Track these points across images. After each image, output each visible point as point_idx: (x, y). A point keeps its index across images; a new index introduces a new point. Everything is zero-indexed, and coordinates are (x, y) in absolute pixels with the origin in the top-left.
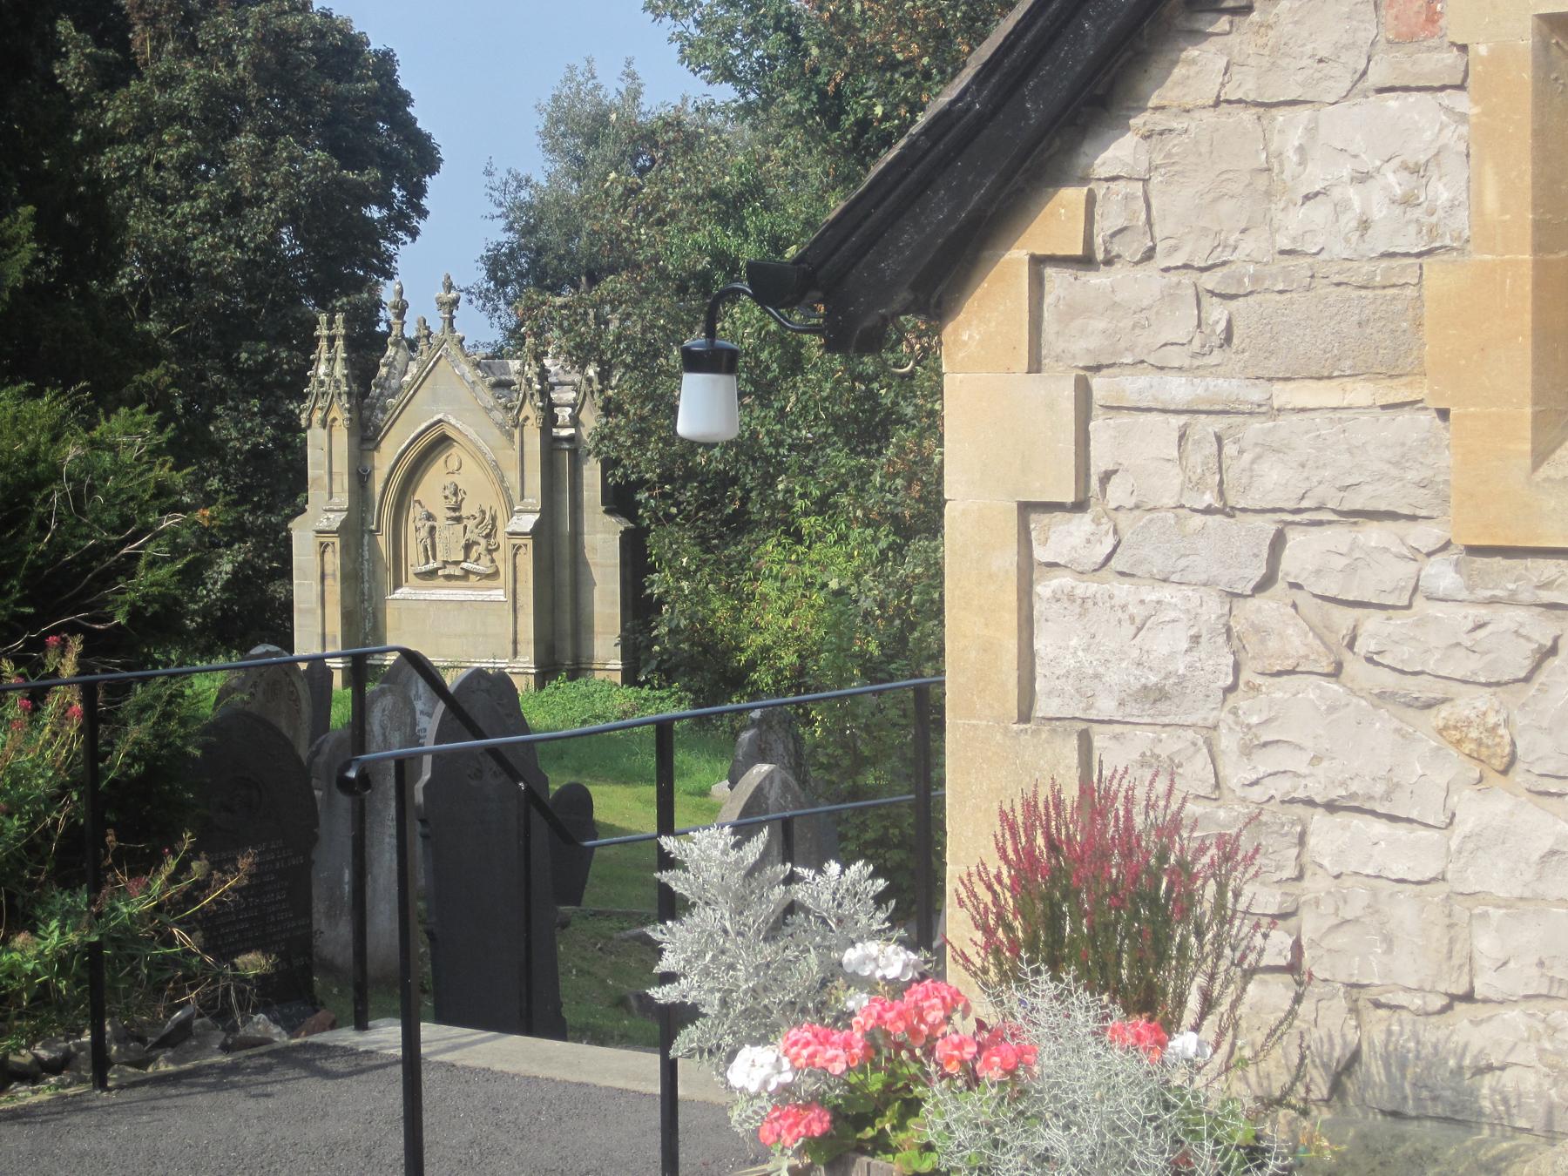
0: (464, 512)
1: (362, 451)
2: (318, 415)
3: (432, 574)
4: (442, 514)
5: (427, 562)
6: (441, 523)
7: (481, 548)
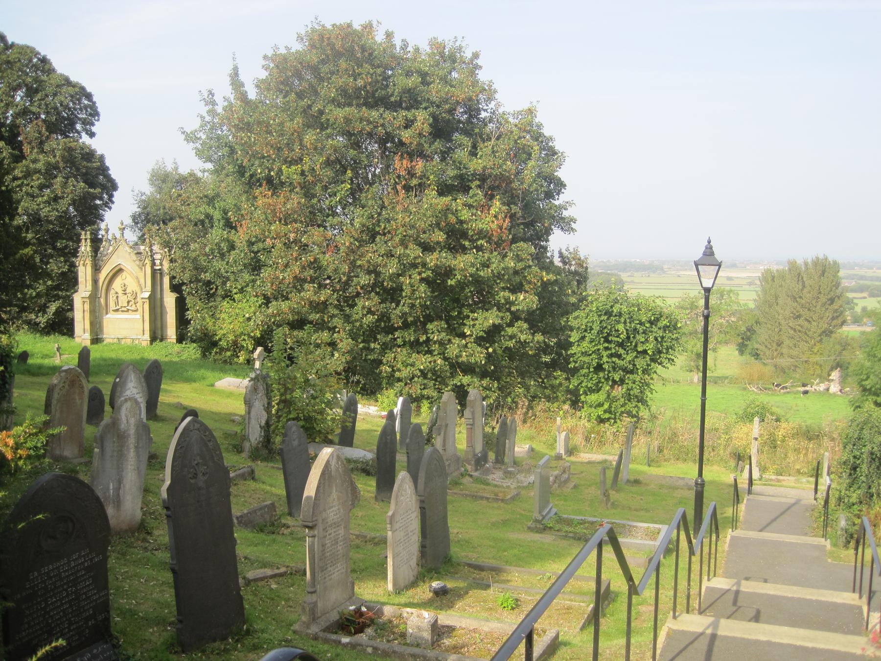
2: (82, 262)
3: (117, 310)
4: (120, 292)
6: (120, 295)
7: (132, 303)
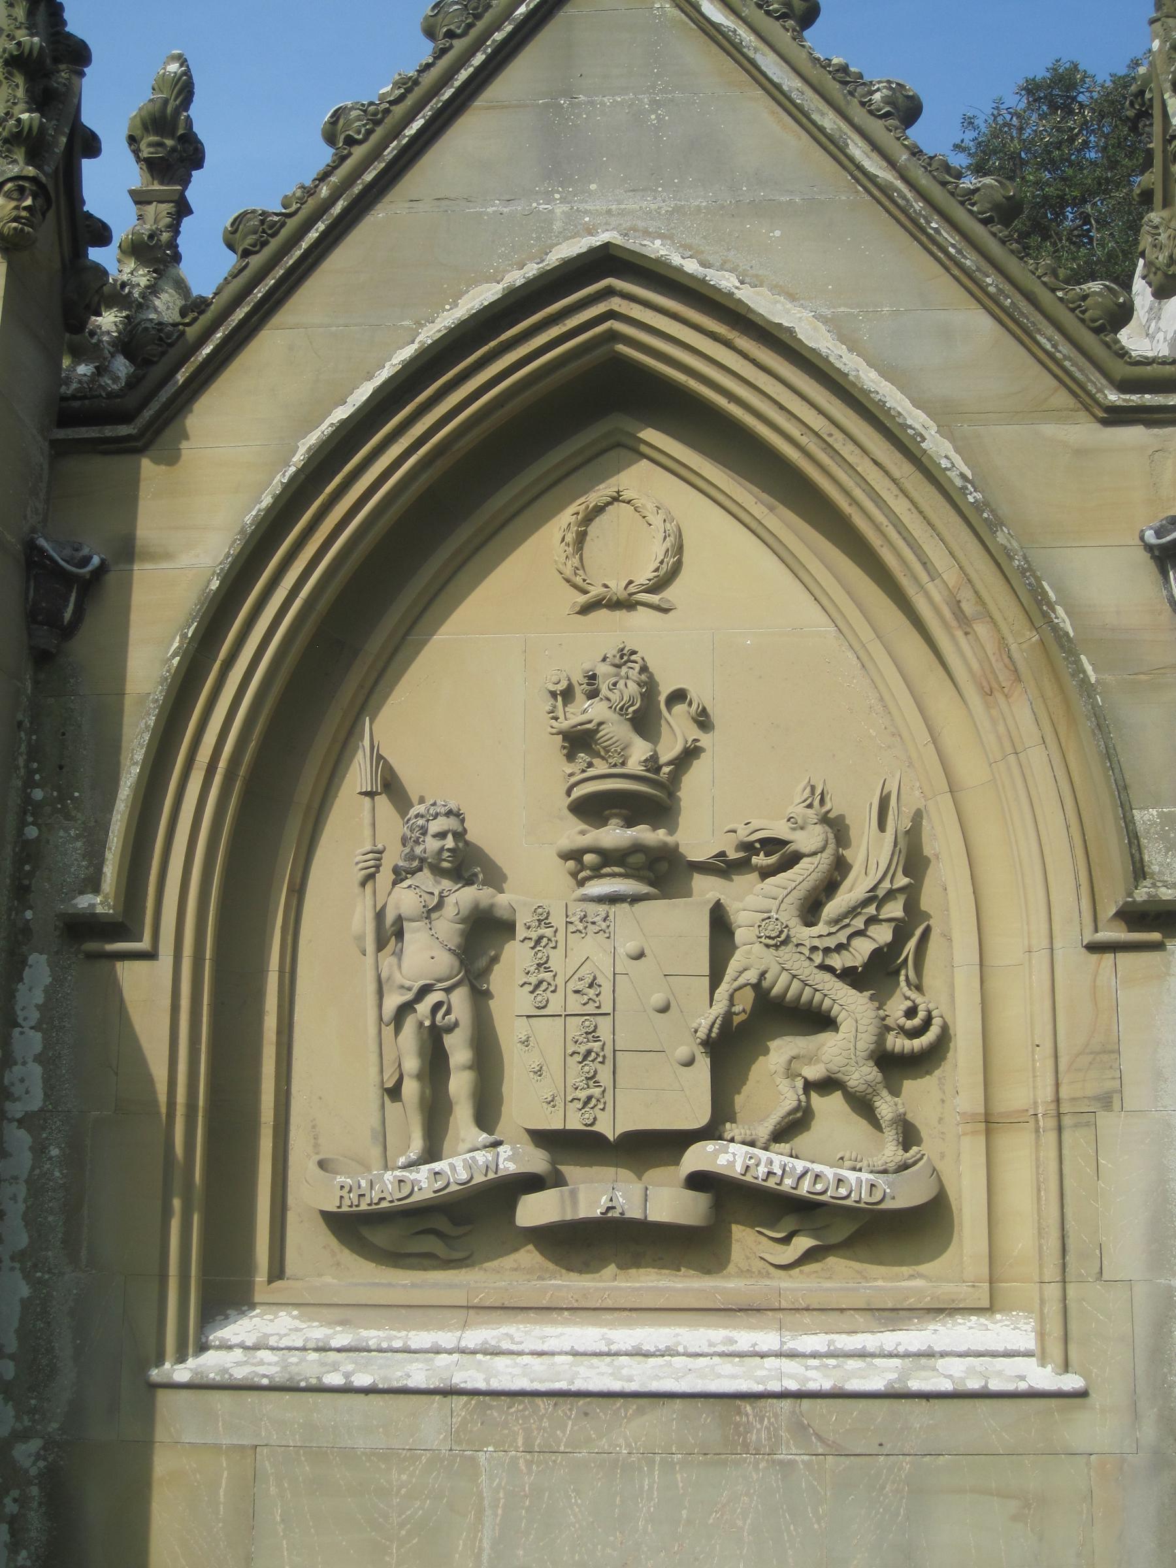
0: (699, 832)
1: (60, 450)
3: (461, 1226)
4: (532, 837)
7: (842, 1050)
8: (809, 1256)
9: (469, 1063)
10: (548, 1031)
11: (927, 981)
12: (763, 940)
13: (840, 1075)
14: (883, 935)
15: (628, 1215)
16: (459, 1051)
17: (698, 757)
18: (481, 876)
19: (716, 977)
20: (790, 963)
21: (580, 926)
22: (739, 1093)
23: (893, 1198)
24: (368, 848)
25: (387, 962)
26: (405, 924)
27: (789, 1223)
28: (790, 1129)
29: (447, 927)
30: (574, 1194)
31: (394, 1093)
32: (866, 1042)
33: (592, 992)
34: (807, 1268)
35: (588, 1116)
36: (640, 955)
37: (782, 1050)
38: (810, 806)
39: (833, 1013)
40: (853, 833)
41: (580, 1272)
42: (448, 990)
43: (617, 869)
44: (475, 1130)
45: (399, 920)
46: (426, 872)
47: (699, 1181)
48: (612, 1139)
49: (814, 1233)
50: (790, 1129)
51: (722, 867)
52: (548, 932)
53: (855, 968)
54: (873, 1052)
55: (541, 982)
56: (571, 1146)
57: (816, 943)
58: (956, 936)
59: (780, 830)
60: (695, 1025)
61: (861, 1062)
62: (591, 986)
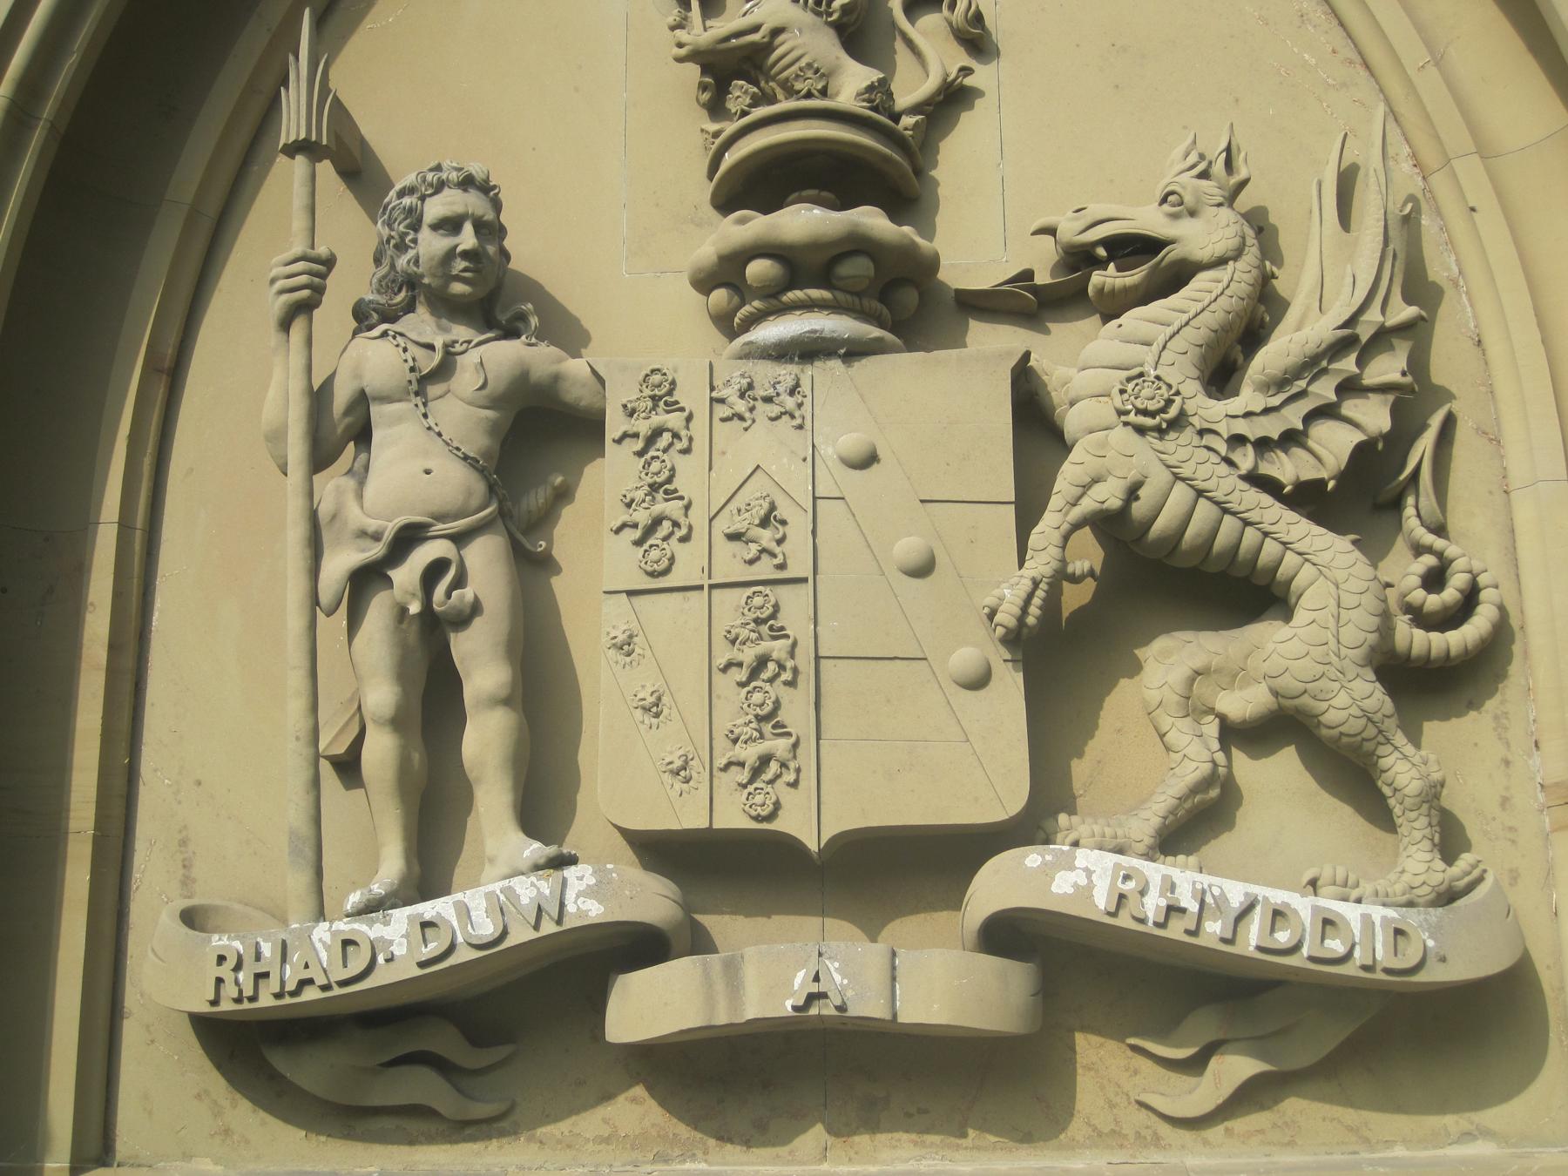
5: (428, 875)
8: (1247, 1097)
9: (504, 693)
10: (674, 624)
11: (1457, 520)
12: (1132, 417)
13: (1306, 700)
14: (1375, 416)
15: (854, 1011)
16: (482, 666)
17: (971, 107)
18: (534, 321)
19: (1028, 509)
20: (1192, 463)
21: (741, 406)
22: (1080, 755)
23: (1443, 960)
24: (298, 248)
25: (332, 484)
26: (376, 410)
27: (1204, 1025)
28: (1196, 824)
29: (461, 412)
30: (732, 968)
31: (349, 767)
32: (1358, 630)
33: (766, 537)
34: (1239, 1124)
35: (762, 802)
36: (868, 460)
37: (1171, 659)
38: (1204, 175)
39: (1282, 573)
40: (1284, 240)
41: (748, 1143)
42: (460, 539)
43: (815, 293)
44: (516, 837)
45: (362, 401)
46: (422, 311)
47: (1007, 935)
48: (813, 846)
49: (1256, 1045)
50: (1196, 824)
51: (1026, 304)
52: (674, 420)
53: (1321, 483)
54: (1373, 649)
55: (657, 522)
56: (724, 868)
57: (1241, 427)
58: (1512, 431)
59: (1149, 220)
60: (990, 601)
61: (1352, 670)
62: (764, 523)
